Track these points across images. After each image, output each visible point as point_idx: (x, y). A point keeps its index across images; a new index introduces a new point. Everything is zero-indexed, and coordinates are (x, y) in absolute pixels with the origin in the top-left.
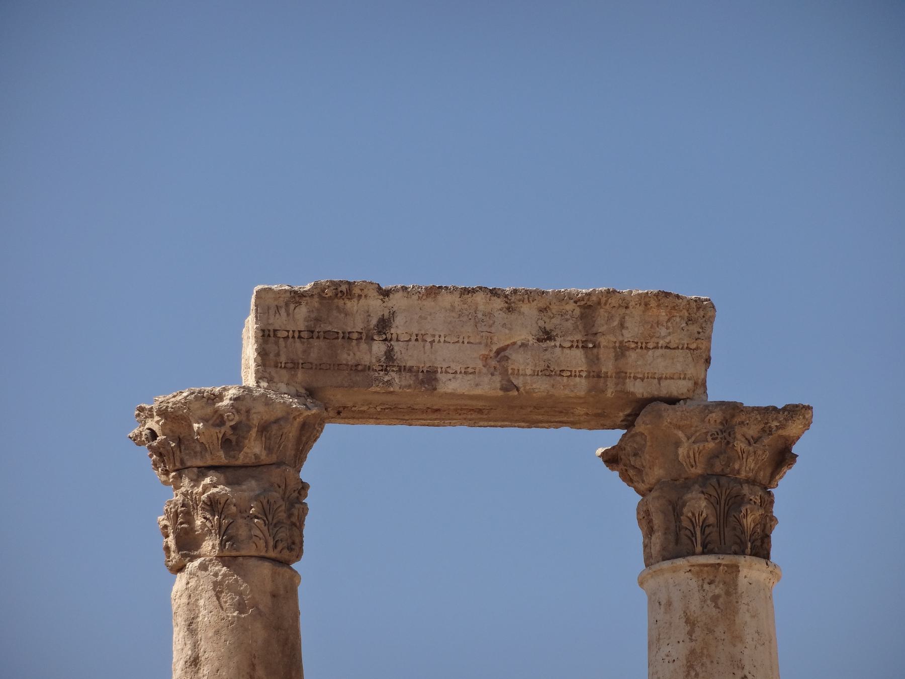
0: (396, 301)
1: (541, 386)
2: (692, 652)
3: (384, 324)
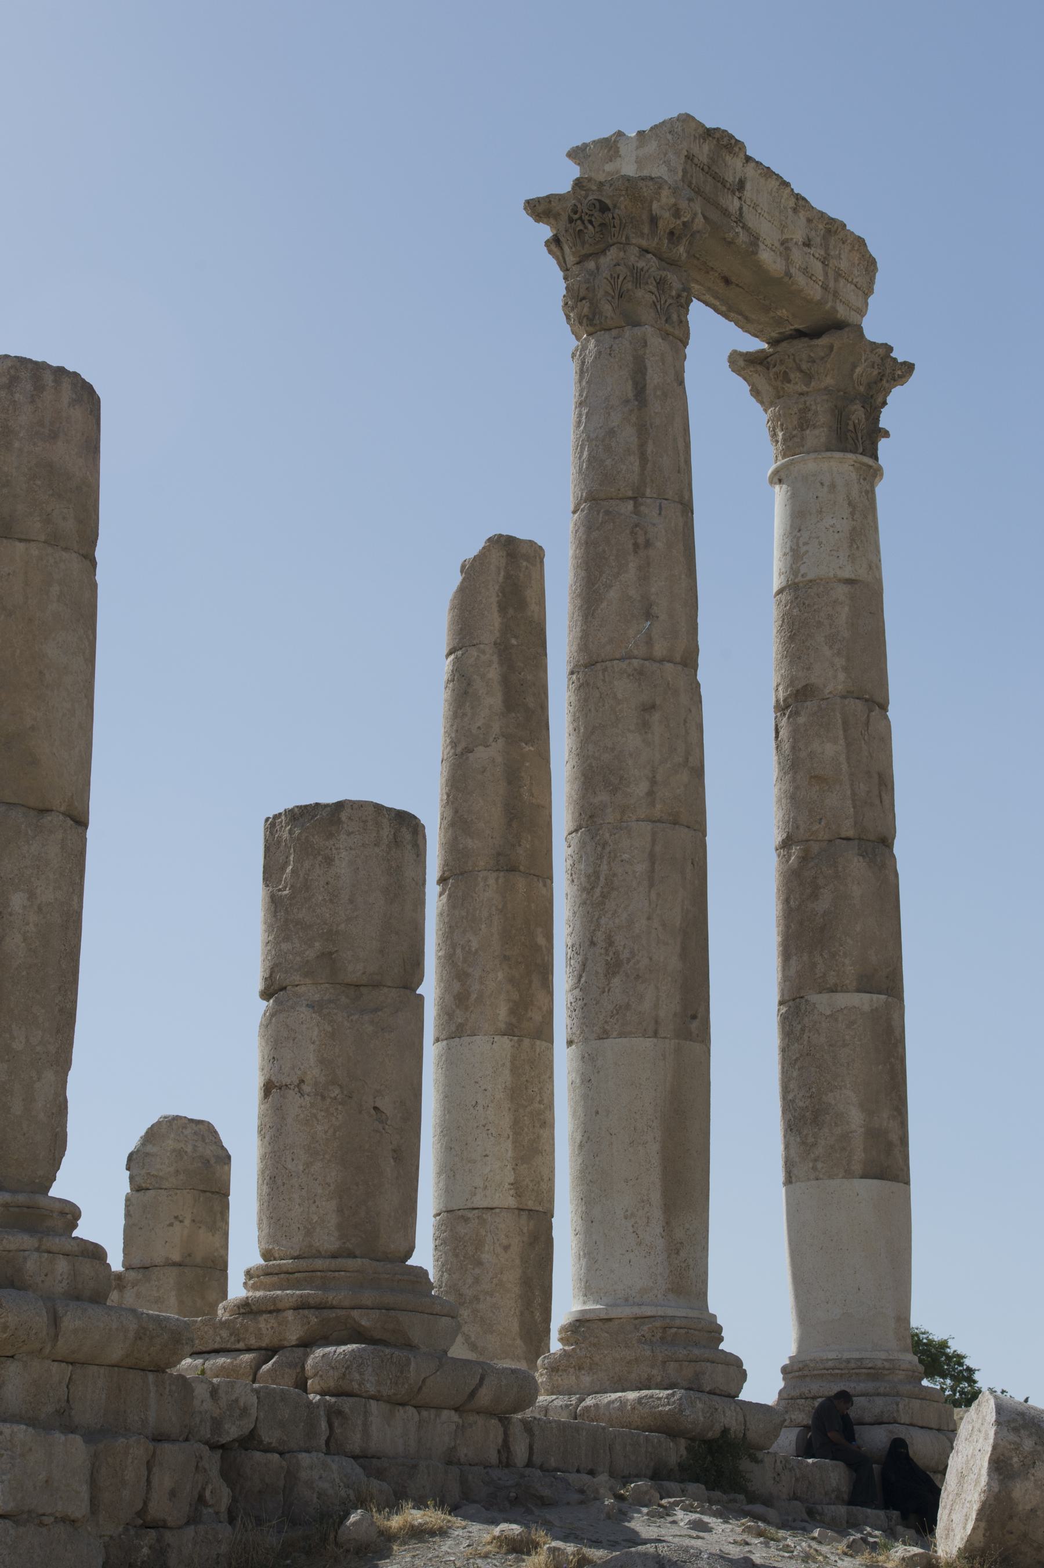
1: (801, 280)
2: (854, 529)
3: (741, 185)
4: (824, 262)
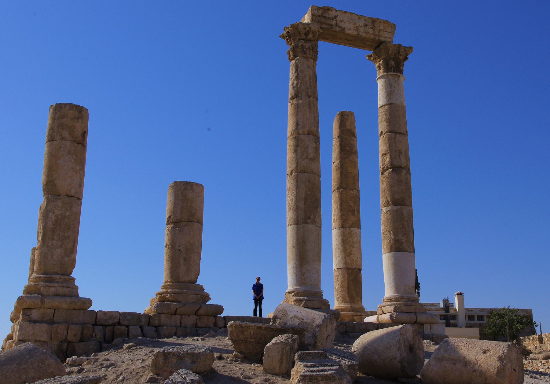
0: (338, 13)
1: (364, 35)
3: (336, 17)
4: (373, 28)
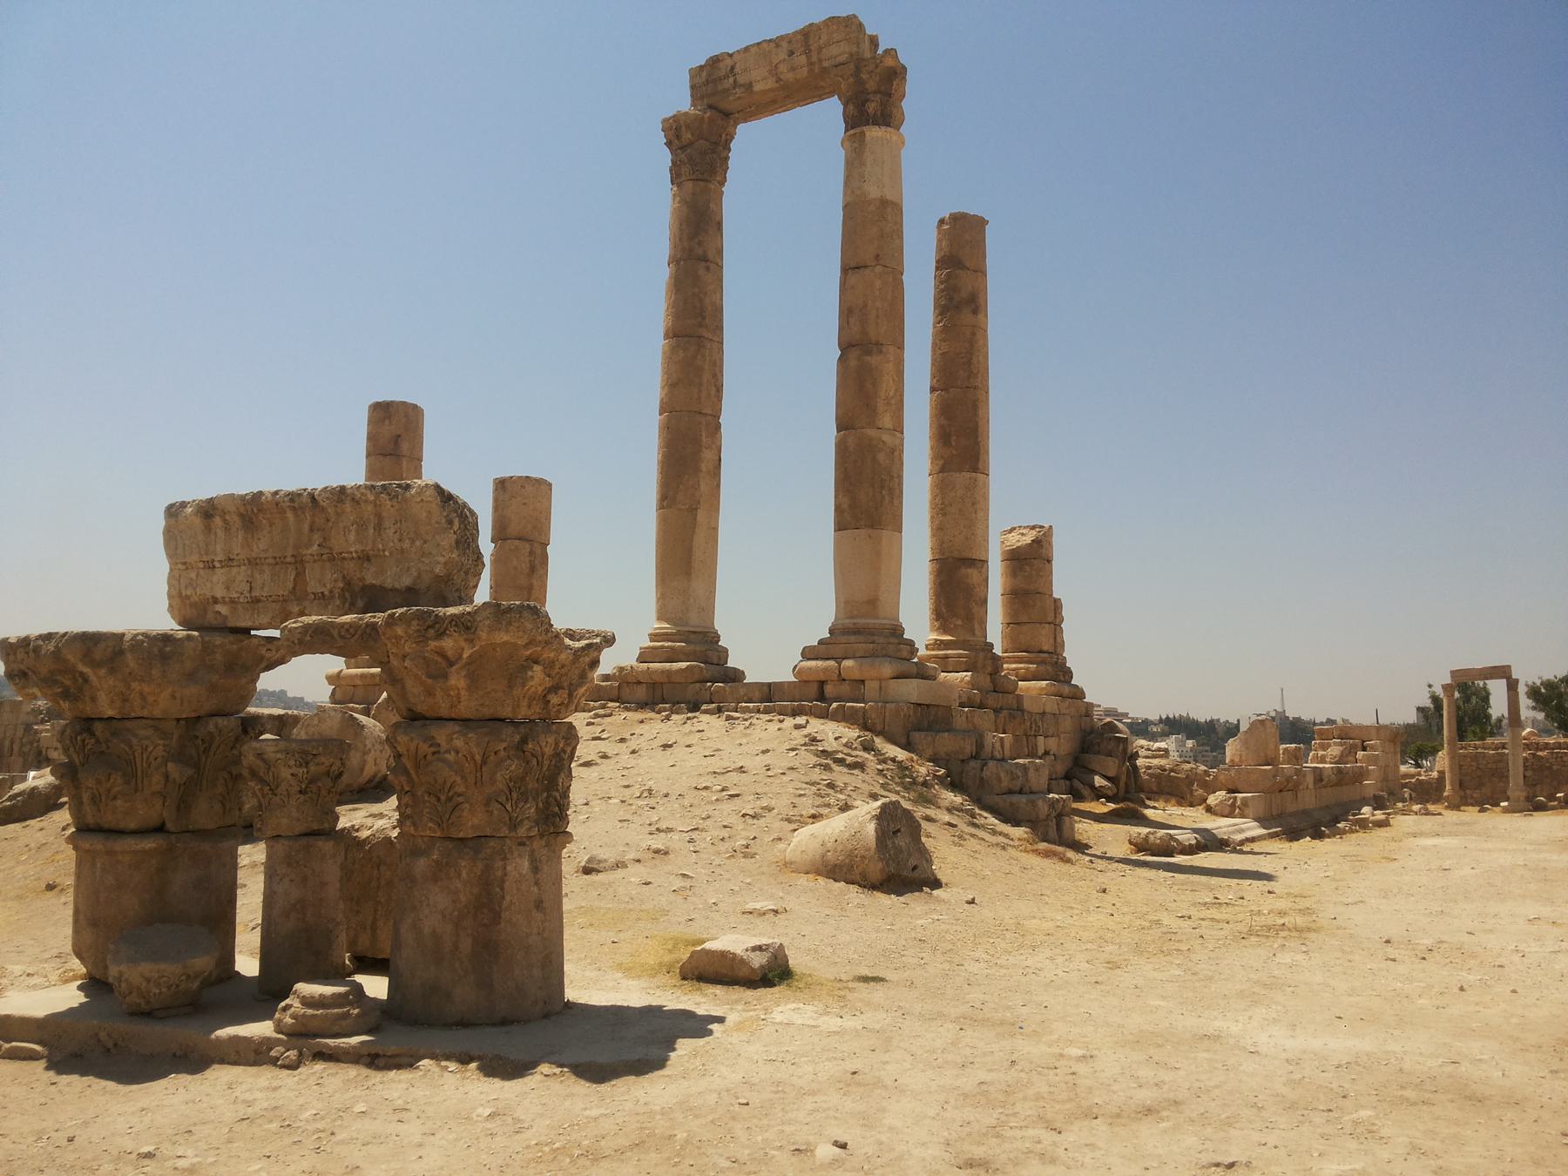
1: (790, 76)
3: (733, 68)
4: (808, 52)
